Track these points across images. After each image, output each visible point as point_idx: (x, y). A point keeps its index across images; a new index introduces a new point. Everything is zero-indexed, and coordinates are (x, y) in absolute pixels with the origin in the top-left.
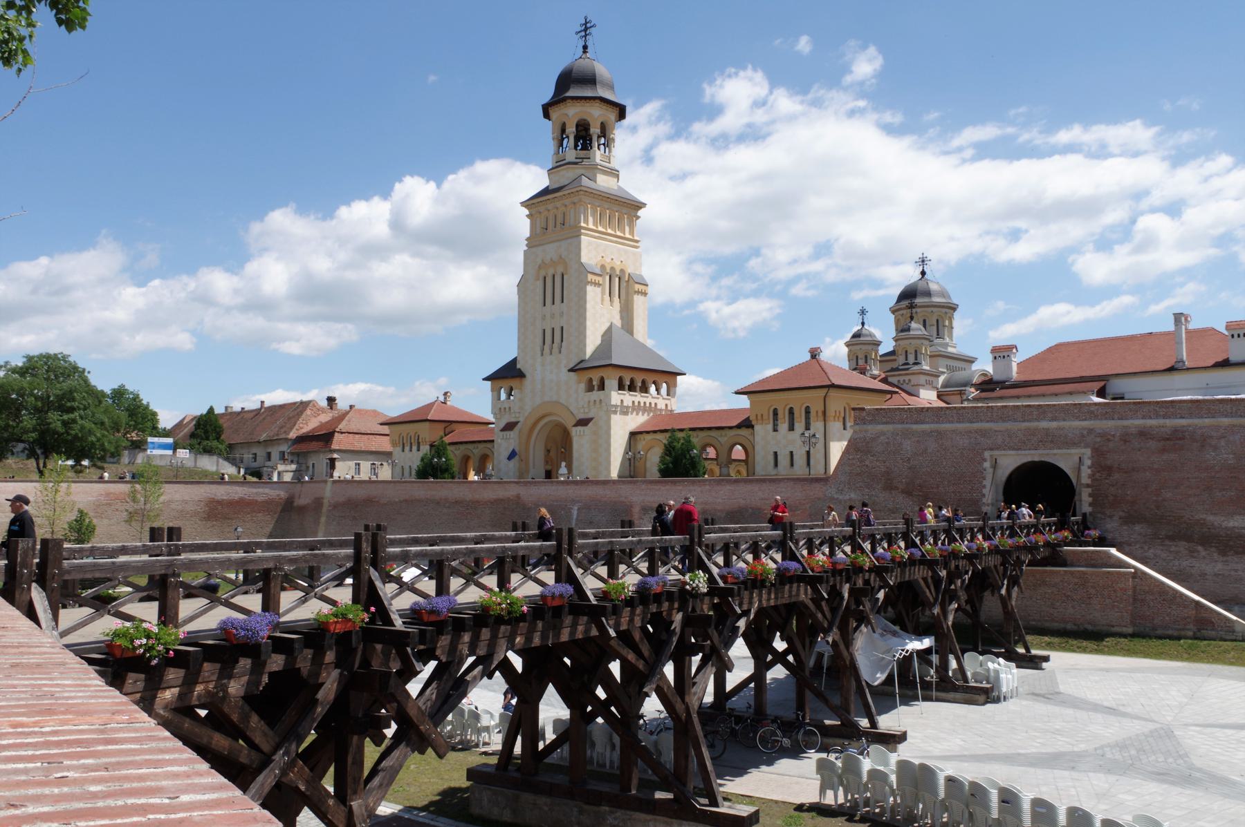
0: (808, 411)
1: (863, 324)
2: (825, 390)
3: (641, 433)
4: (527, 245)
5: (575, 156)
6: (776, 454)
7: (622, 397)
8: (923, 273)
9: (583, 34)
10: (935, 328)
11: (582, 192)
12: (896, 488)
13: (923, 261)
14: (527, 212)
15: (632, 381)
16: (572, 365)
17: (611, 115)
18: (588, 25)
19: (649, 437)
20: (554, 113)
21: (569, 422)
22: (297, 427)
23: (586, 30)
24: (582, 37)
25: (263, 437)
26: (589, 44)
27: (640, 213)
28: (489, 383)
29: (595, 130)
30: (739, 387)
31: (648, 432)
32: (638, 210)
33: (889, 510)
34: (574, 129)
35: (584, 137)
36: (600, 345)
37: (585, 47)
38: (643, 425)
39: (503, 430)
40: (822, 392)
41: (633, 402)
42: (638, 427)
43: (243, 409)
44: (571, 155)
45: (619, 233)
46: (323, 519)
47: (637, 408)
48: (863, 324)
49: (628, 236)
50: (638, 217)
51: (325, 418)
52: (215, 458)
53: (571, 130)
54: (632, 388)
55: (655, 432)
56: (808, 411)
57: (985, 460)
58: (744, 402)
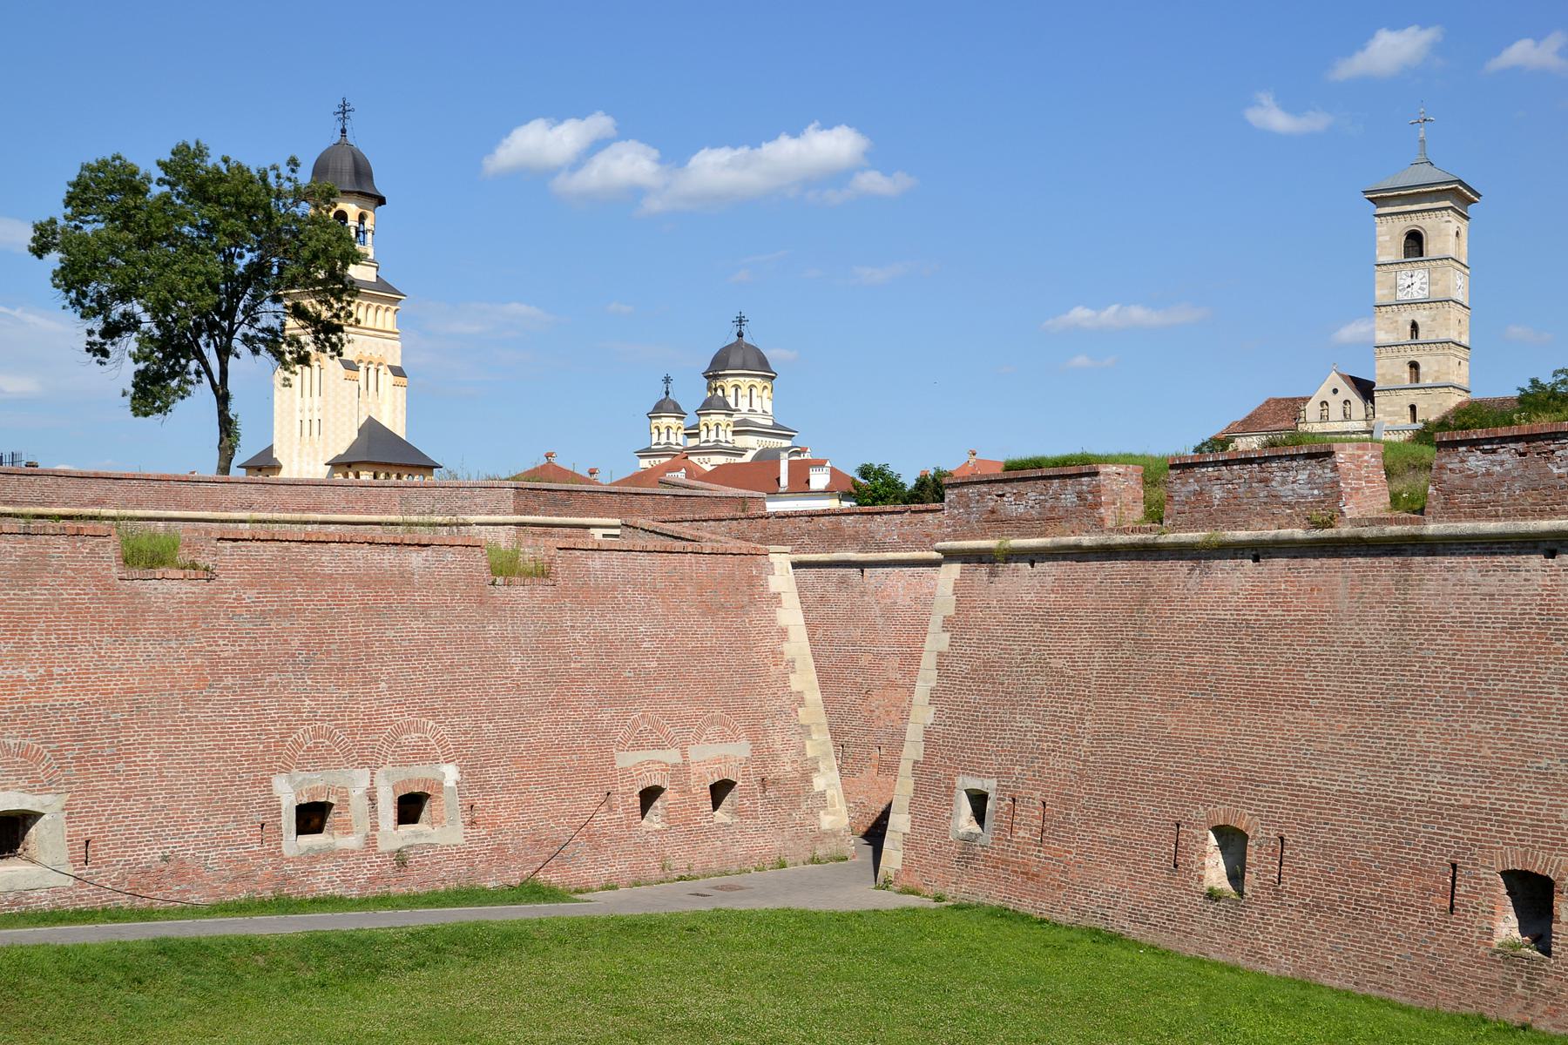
8: (740, 335)
13: (740, 321)
16: (329, 458)
24: (339, 119)
37: (343, 131)
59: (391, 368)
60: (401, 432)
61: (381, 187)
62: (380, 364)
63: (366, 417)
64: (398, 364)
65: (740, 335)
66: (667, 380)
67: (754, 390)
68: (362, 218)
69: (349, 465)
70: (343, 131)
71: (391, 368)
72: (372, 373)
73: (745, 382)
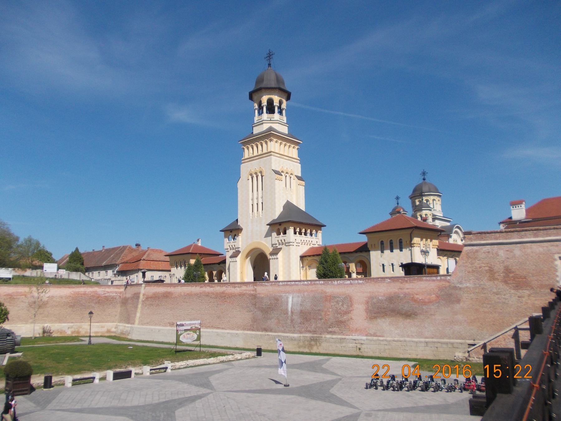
0: (401, 242)
1: (398, 204)
2: (411, 230)
3: (306, 256)
5: (267, 117)
6: (383, 265)
7: (296, 238)
8: (424, 179)
9: (268, 58)
10: (432, 204)
12: (497, 279)
15: (300, 230)
16: (268, 222)
18: (271, 54)
19: (309, 258)
21: (267, 253)
22: (120, 258)
23: (269, 57)
25: (104, 264)
28: (223, 233)
29: (276, 103)
30: (362, 230)
31: (310, 256)
33: (494, 293)
34: (266, 104)
36: (283, 211)
38: (306, 252)
39: (231, 257)
40: (409, 231)
41: (301, 240)
42: (303, 254)
43: (93, 250)
44: (265, 116)
46: (140, 306)
47: (303, 243)
48: (398, 204)
51: (135, 254)
52: (79, 273)
53: (264, 103)
54: (300, 233)
55: (314, 256)
56: (401, 242)
57: (555, 260)
58: (364, 239)
59: (297, 177)
60: (304, 211)
61: (288, 88)
62: (292, 174)
63: (286, 201)
64: (300, 175)
65: (424, 179)
66: (398, 198)
67: (434, 201)
68: (281, 103)
69: (280, 224)
71: (297, 177)
72: (288, 178)
73: (431, 198)
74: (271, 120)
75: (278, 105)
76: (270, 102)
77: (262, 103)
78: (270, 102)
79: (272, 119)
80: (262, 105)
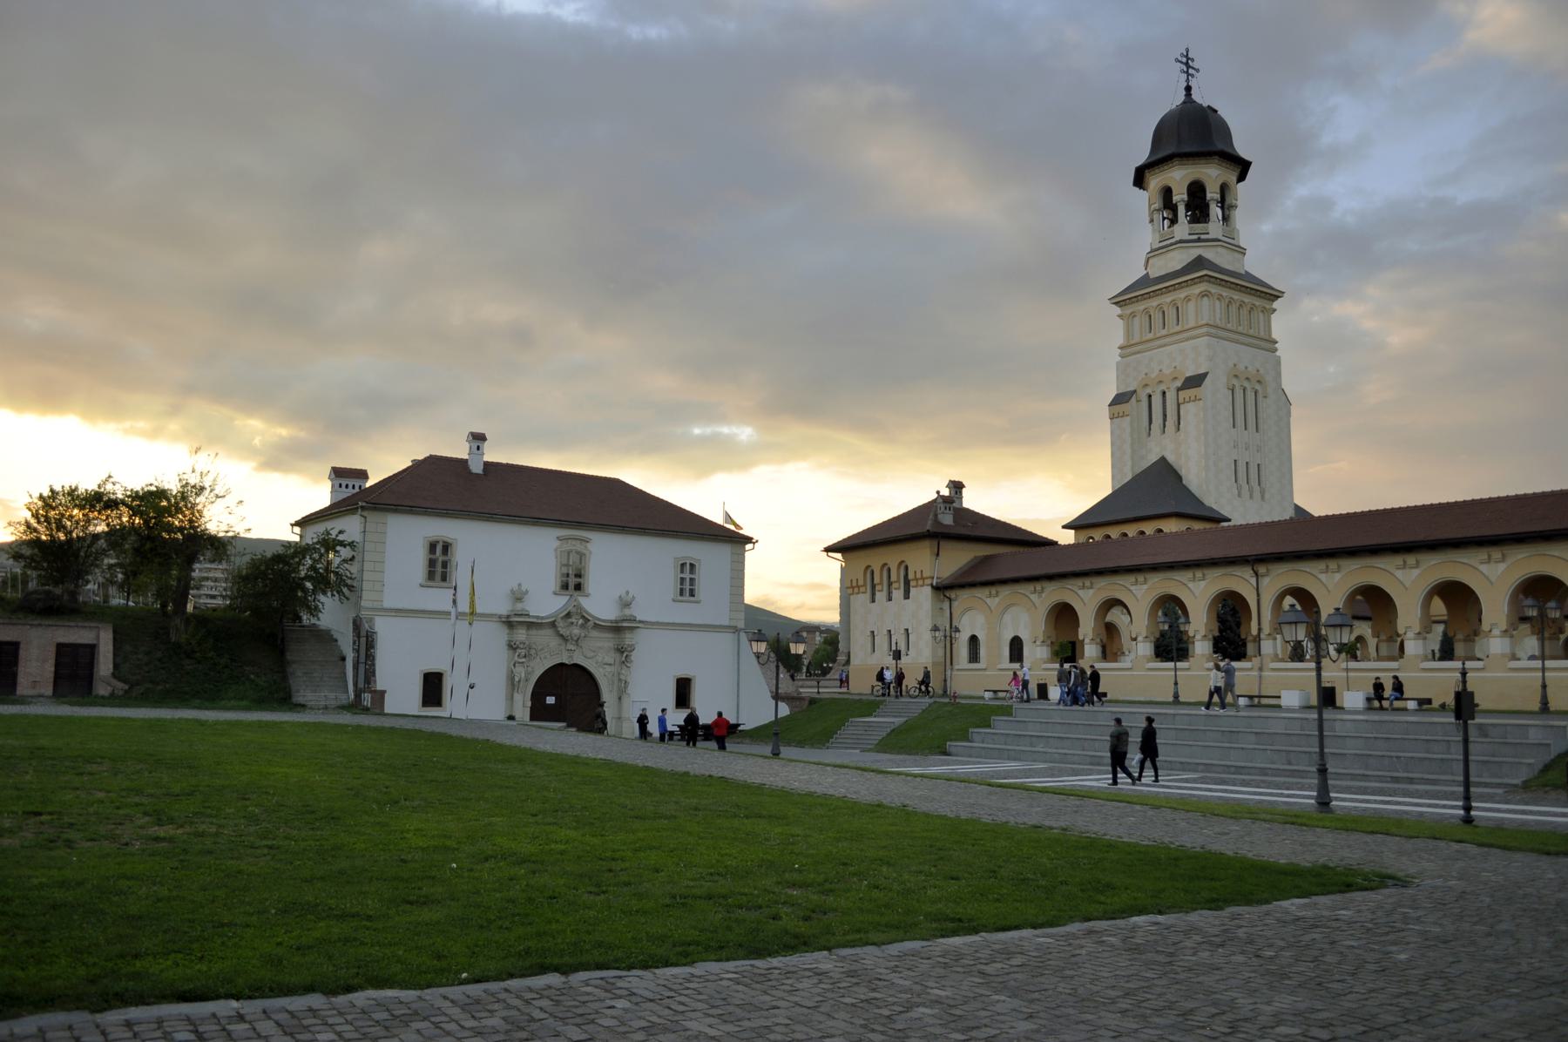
4: (1120, 356)
5: (1188, 232)
11: (1206, 278)
14: (1118, 310)
17: (1232, 177)
20: (1155, 181)
26: (1193, 83)
27: (1276, 305)
29: (1212, 194)
32: (1273, 301)
34: (1185, 197)
35: (1198, 205)
37: (1188, 89)
44: (1183, 229)
45: (1251, 332)
49: (1262, 334)
50: (1275, 310)
53: (1180, 196)
61: (1242, 148)
70: (1188, 89)
74: (1199, 240)
75: (1218, 196)
76: (1197, 191)
77: (1174, 193)
78: (1197, 191)
79: (1203, 237)
80: (1174, 202)
